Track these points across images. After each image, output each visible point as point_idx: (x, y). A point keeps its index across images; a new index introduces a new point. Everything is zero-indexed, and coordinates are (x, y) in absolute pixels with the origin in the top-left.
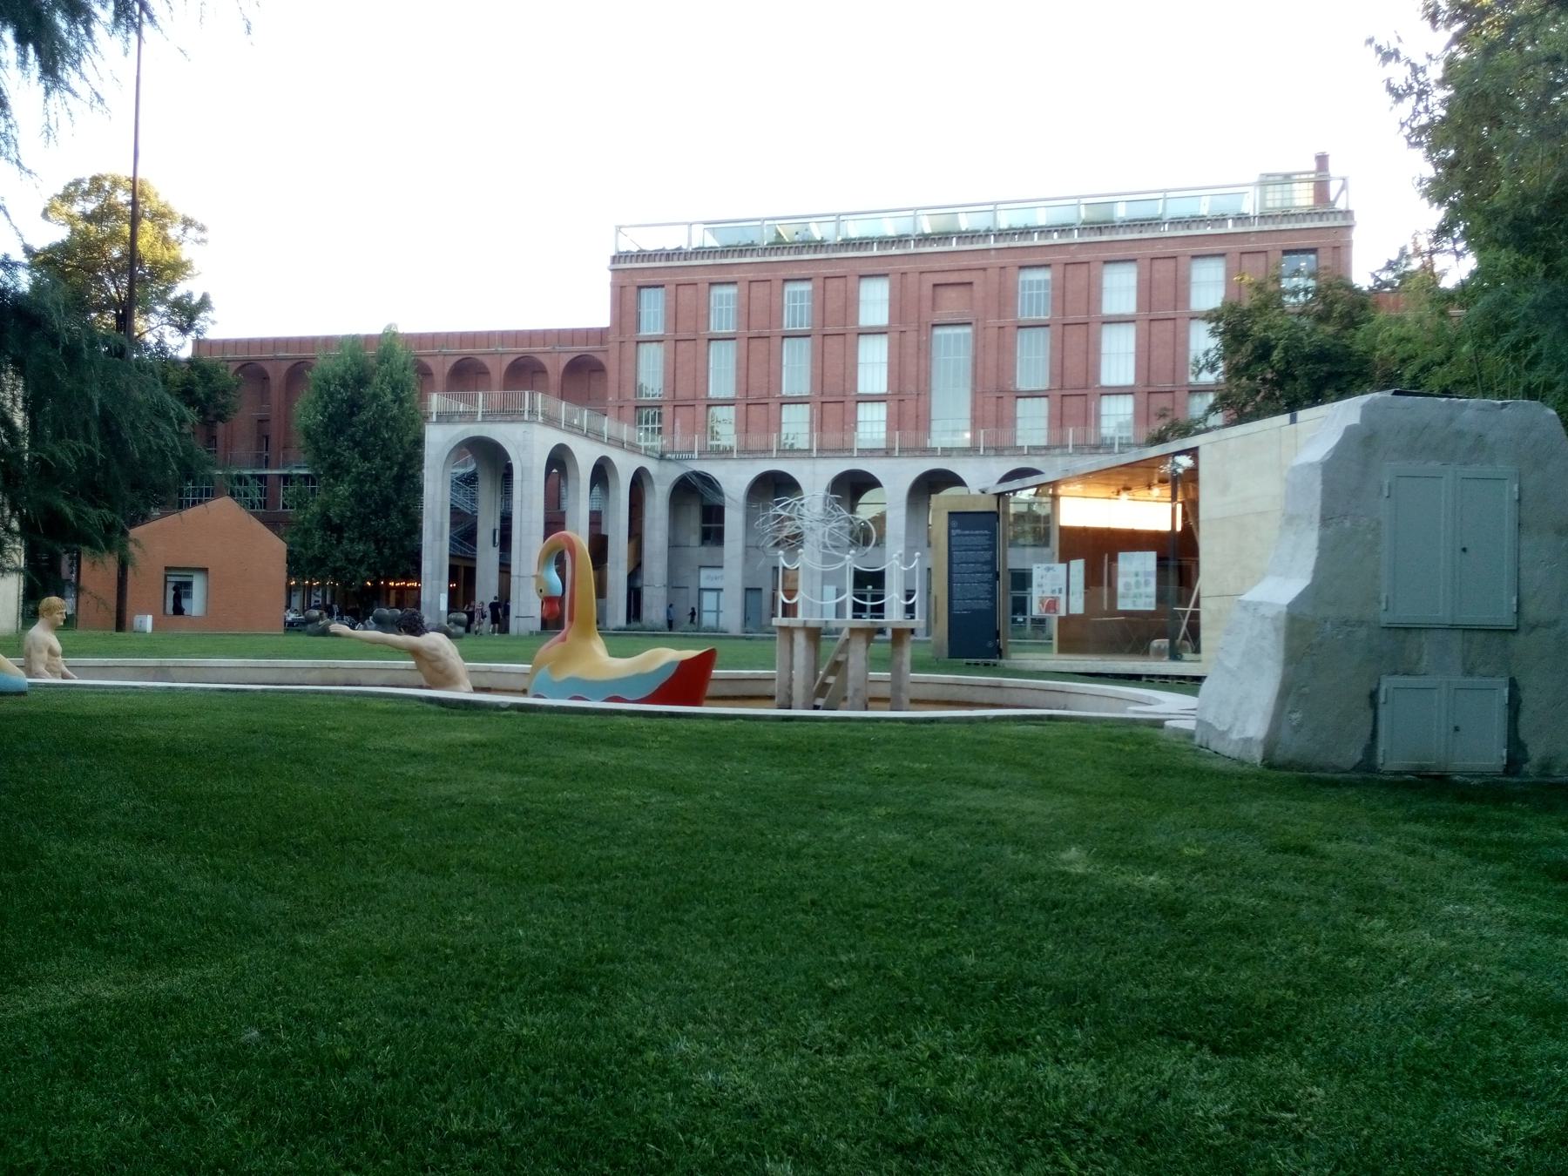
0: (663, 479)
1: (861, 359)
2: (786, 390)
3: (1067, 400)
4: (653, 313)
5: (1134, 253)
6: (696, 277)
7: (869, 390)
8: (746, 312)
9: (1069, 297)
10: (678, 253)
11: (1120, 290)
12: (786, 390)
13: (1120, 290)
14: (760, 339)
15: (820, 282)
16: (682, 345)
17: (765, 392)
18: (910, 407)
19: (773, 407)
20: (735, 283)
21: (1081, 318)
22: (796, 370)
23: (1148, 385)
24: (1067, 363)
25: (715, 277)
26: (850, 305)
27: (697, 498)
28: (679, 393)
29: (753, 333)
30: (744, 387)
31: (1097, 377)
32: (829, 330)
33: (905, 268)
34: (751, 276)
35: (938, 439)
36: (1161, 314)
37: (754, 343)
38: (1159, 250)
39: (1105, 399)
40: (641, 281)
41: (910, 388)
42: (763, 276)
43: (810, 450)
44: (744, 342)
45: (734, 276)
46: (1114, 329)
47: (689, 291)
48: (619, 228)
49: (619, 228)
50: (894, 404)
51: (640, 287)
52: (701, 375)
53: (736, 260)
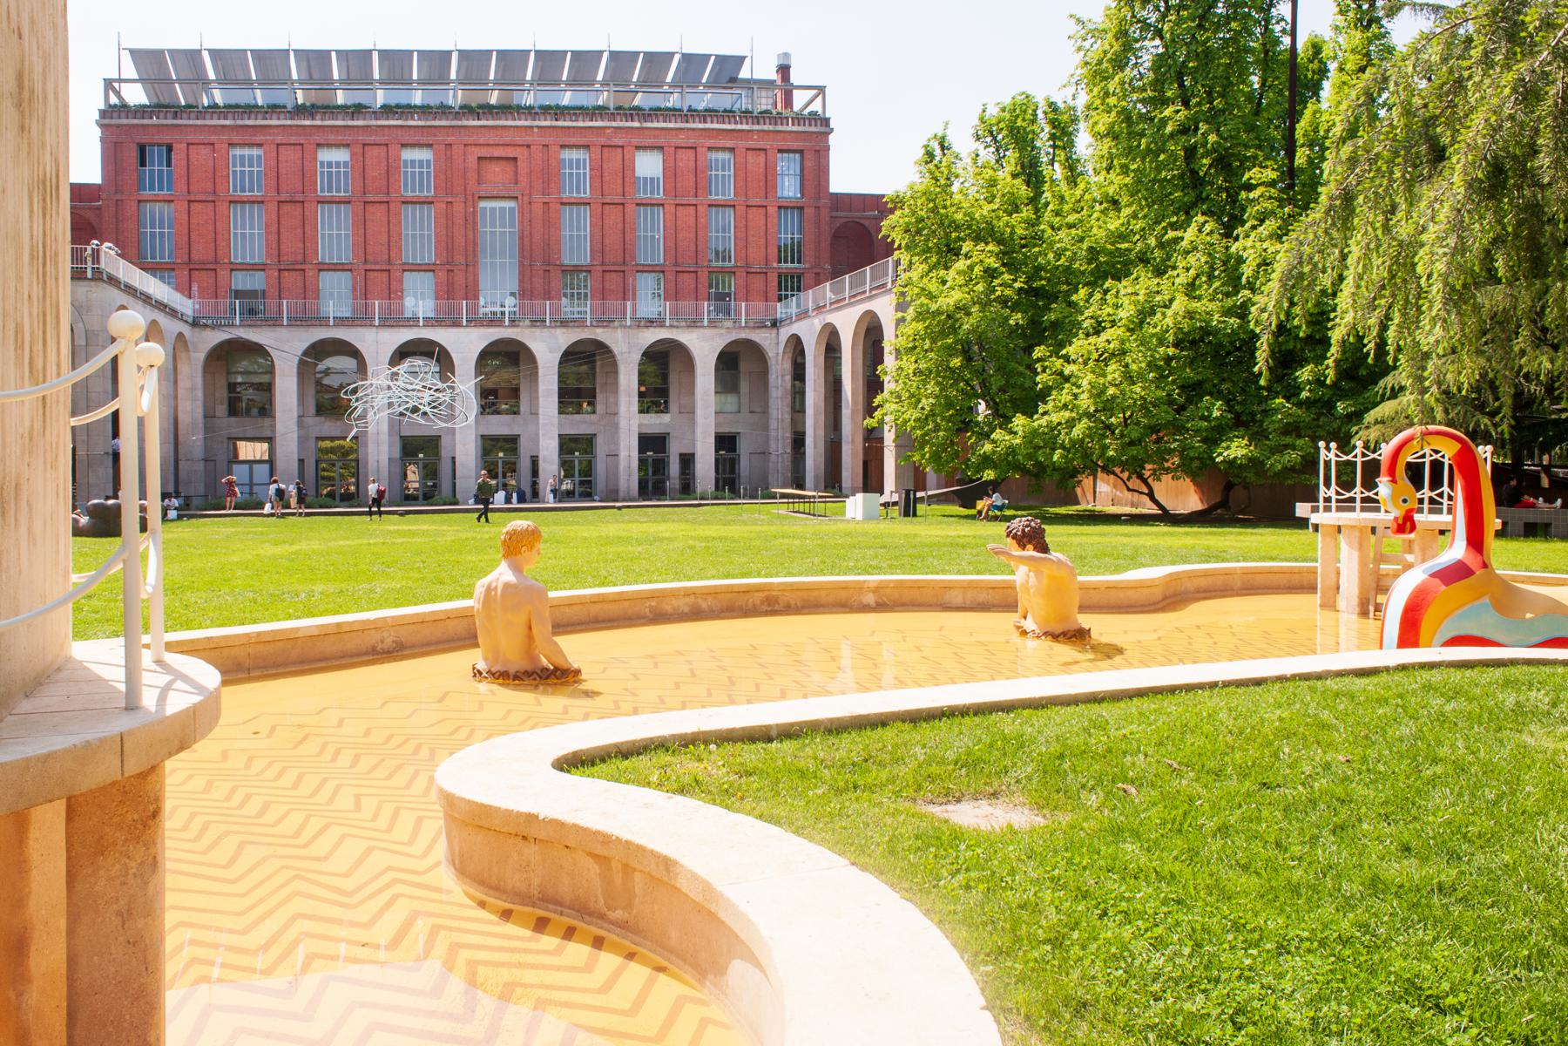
3: (607, 275)
6: (213, 138)
9: (606, 179)
12: (323, 255)
17: (300, 258)
19: (310, 274)
21: (618, 199)
22: (334, 235)
23: (676, 264)
24: (607, 241)
30: (275, 252)
31: (634, 259)
32: (370, 198)
34: (279, 139)
35: (485, 306)
36: (685, 200)
37: (286, 208)
42: (293, 139)
44: (273, 207)
45: (259, 138)
50: (442, 275)
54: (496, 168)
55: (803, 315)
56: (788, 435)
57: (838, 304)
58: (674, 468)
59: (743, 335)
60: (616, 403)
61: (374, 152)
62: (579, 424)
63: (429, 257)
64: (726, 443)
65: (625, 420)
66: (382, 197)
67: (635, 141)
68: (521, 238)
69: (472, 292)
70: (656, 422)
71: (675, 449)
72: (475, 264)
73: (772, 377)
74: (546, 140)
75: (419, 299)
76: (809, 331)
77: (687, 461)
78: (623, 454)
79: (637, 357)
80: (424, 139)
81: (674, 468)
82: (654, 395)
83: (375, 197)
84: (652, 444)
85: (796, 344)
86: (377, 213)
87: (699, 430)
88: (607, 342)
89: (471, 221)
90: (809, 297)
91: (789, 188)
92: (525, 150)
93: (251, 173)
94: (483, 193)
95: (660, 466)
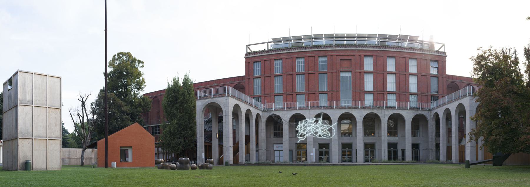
0: (264, 116)
4: (258, 68)
5: (394, 55)
6: (270, 58)
8: (285, 68)
10: (264, 51)
11: (391, 65)
13: (391, 65)
14: (289, 75)
16: (267, 78)
19: (294, 95)
20: (281, 59)
25: (276, 58)
27: (275, 123)
28: (266, 93)
29: (287, 73)
34: (286, 57)
38: (401, 55)
39: (388, 95)
40: (254, 60)
44: (285, 76)
45: (281, 57)
46: (390, 75)
47: (268, 62)
48: (247, 46)
49: (247, 46)
51: (254, 62)
52: (272, 87)
53: (282, 52)
54: (345, 62)
55: (439, 106)
56: (434, 143)
57: (450, 102)
58: (399, 153)
59: (420, 112)
60: (381, 133)
61: (311, 59)
62: (370, 140)
63: (326, 89)
64: (415, 146)
65: (384, 137)
67: (387, 55)
68: (353, 83)
69: (338, 99)
70: (393, 139)
71: (399, 148)
72: (339, 91)
73: (429, 126)
74: (360, 54)
75: (323, 101)
76: (441, 112)
77: (403, 152)
78: (383, 149)
79: (387, 118)
80: (325, 54)
81: (399, 153)
82: (392, 132)
83: (311, 73)
84: (392, 146)
85: (437, 116)
87: (407, 142)
88: (380, 115)
89: (338, 78)
90: (441, 101)
91: (434, 71)
92: (354, 57)
94: (341, 70)
95: (395, 153)
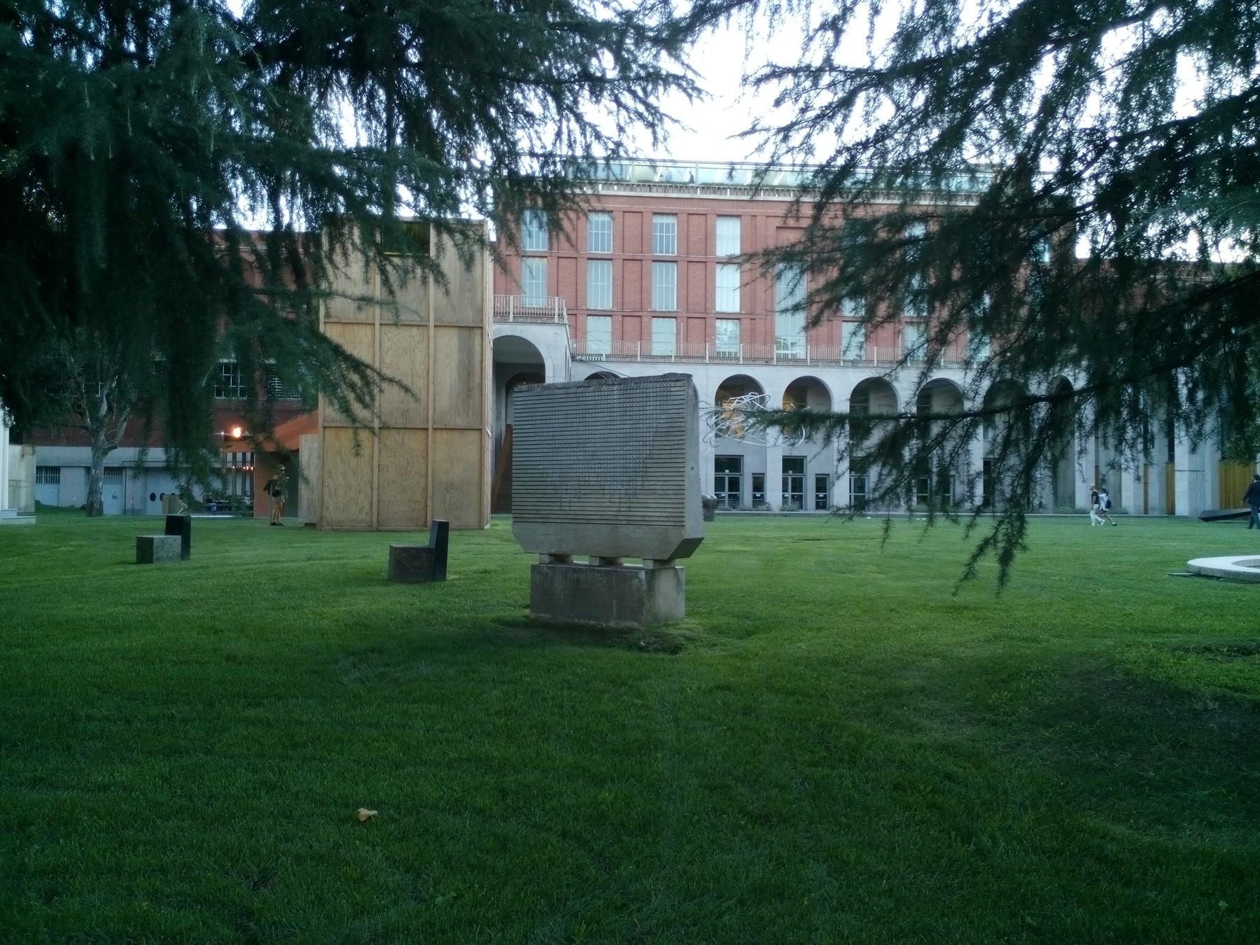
1: (718, 283)
2: (592, 305)
7: (724, 310)
12: (658, 304)
15: (684, 217)
17: (638, 307)
18: (760, 325)
19: (645, 319)
22: (665, 289)
26: (708, 239)
30: (620, 301)
32: (693, 257)
33: (755, 211)
34: (626, 207)
41: (760, 309)
42: (635, 208)
43: (704, 358)
44: (619, 263)
50: (746, 322)
66: (701, 258)
86: (697, 270)
93: (597, 234)
